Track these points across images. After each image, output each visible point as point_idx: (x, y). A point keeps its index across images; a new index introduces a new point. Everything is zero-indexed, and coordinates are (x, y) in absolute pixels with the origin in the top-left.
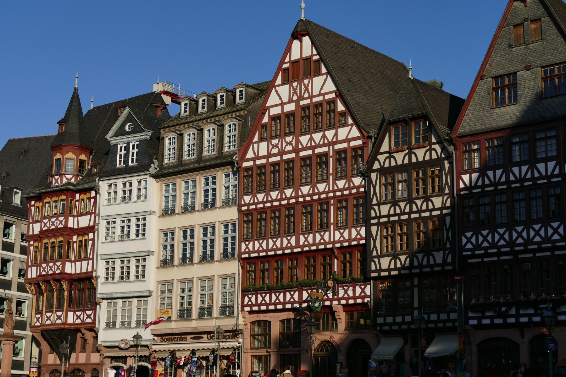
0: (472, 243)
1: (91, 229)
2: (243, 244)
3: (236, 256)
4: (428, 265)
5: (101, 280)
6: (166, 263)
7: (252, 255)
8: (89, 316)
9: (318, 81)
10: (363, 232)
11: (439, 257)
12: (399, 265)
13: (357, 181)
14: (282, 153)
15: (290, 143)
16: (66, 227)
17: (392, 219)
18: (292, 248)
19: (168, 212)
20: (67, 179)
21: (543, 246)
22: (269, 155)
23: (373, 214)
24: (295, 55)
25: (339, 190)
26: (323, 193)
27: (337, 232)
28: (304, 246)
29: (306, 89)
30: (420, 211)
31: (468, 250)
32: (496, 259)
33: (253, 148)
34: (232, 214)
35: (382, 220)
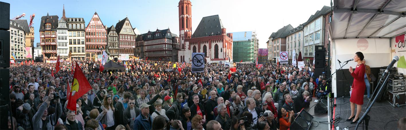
1: (56, 37)
5: (58, 46)
13: (106, 37)
14: (93, 31)
16: (51, 37)
22: (91, 31)
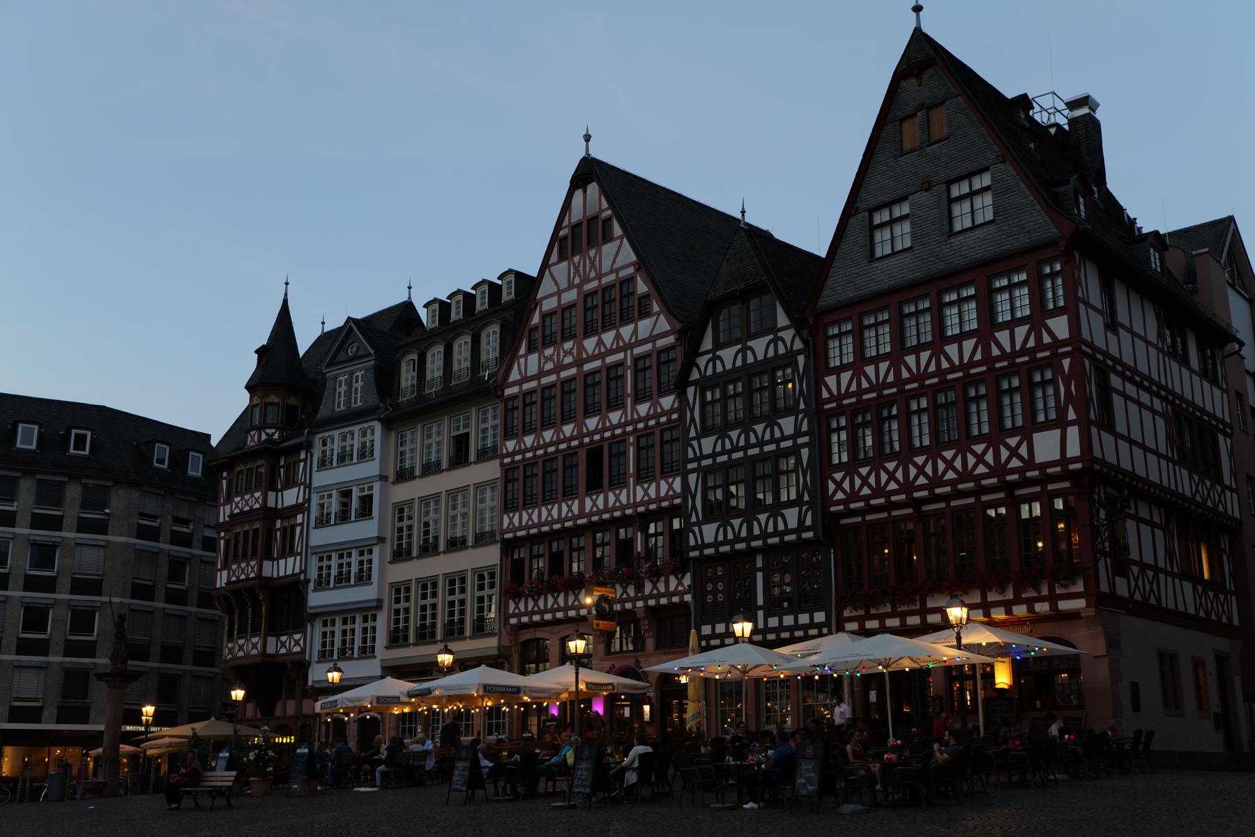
0: (844, 491)
2: (505, 517)
3: (498, 537)
4: (776, 533)
5: (311, 586)
6: (401, 554)
7: (519, 534)
8: (297, 643)
9: (608, 249)
10: (677, 485)
11: (792, 515)
12: (730, 536)
14: (559, 368)
15: (570, 352)
17: (720, 459)
18: (574, 518)
19: (404, 475)
20: (267, 434)
21: (960, 487)
22: (542, 373)
23: (691, 455)
24: (577, 213)
25: (640, 420)
26: (617, 426)
27: (638, 488)
28: (591, 514)
29: (593, 265)
30: (761, 443)
31: (839, 502)
32: (885, 515)
33: (519, 365)
34: (491, 470)
35: (705, 463)
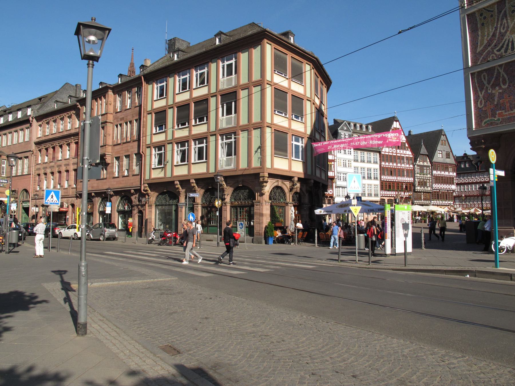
10: (412, 179)
11: (429, 188)
13: (411, 166)
14: (392, 153)
22: (389, 152)
